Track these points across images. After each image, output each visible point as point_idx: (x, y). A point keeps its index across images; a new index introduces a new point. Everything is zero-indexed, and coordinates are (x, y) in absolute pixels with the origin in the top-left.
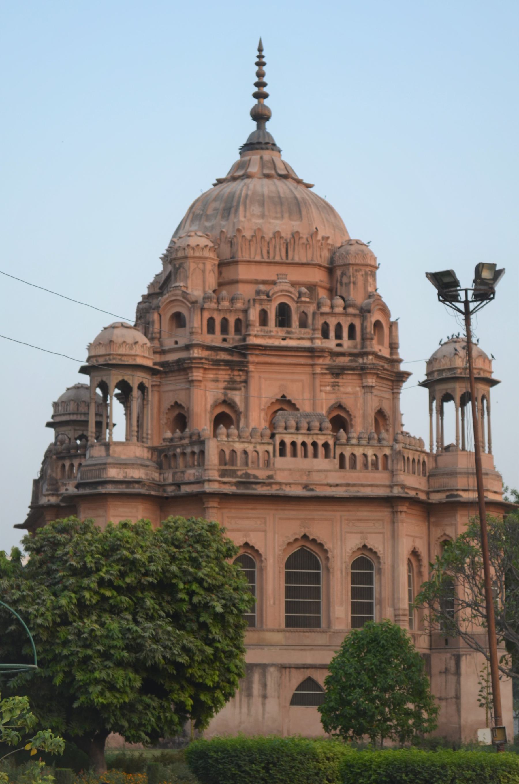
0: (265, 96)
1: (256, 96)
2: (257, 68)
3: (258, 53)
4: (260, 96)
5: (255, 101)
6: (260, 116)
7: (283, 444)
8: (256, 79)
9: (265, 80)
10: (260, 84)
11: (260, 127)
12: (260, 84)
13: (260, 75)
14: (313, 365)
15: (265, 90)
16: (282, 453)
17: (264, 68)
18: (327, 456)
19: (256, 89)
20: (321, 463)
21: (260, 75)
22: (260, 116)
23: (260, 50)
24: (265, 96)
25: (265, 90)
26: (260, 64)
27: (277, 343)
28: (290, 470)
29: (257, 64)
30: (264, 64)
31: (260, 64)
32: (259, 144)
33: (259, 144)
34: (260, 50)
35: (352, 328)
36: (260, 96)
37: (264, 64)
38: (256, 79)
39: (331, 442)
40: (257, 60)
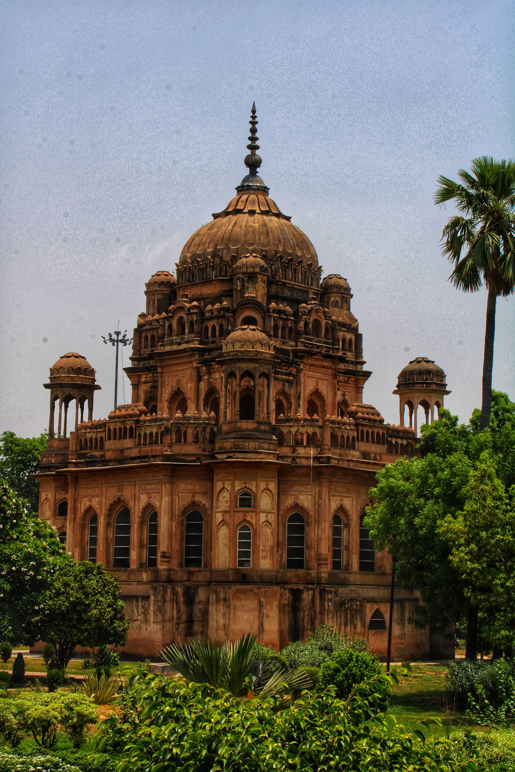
0: (257, 148)
1: (249, 147)
2: (251, 126)
3: (251, 114)
4: (253, 148)
5: (249, 152)
6: (253, 164)
7: (109, 430)
8: (250, 135)
9: (257, 135)
10: (253, 139)
11: (253, 173)
12: (253, 139)
13: (253, 131)
14: (191, 362)
15: (257, 143)
16: (109, 439)
17: (256, 126)
18: (131, 437)
19: (250, 142)
20: (128, 443)
21: (253, 131)
22: (253, 164)
23: (254, 112)
24: (257, 148)
25: (257, 143)
26: (254, 123)
27: (175, 347)
28: (112, 450)
29: (251, 122)
30: (257, 123)
31: (254, 123)
32: (251, 187)
33: (251, 187)
34: (254, 112)
35: (221, 326)
36: (253, 148)
37: (257, 123)
38: (250, 135)
39: (133, 426)
40: (251, 119)
